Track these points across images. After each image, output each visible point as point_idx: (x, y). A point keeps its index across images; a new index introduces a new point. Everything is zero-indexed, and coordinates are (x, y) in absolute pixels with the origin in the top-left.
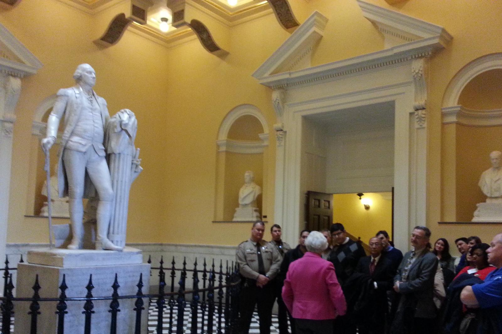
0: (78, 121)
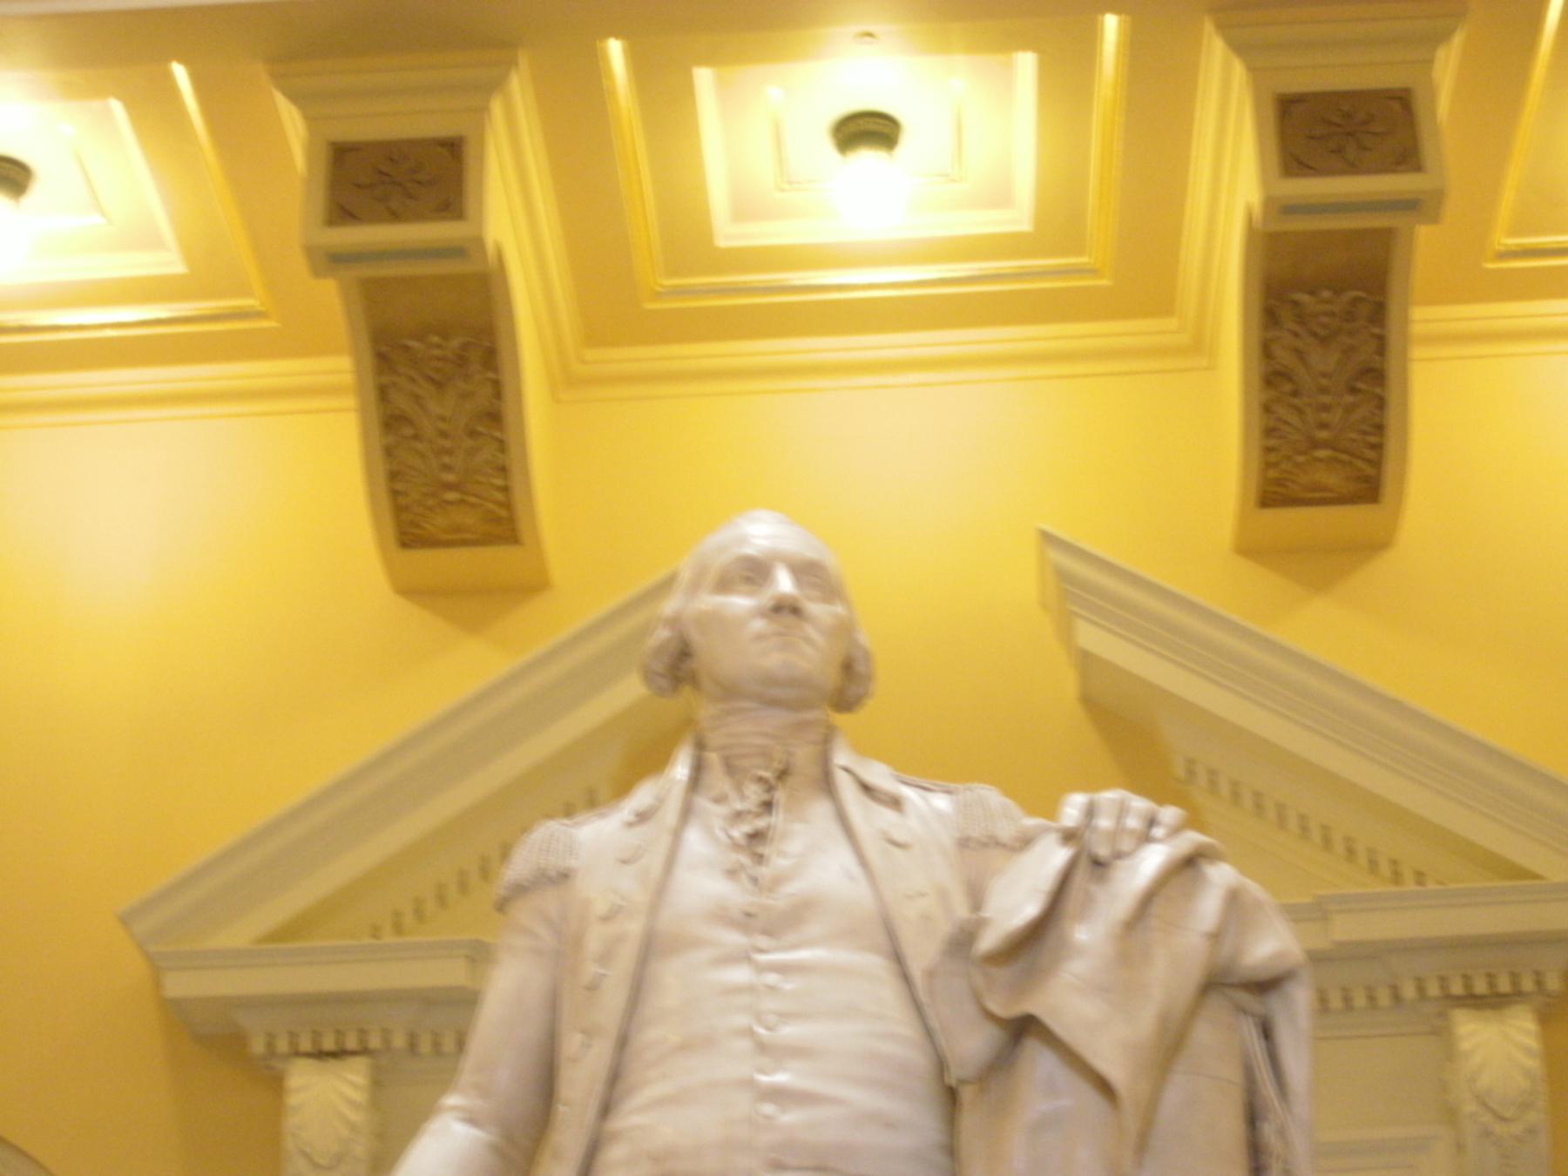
0: (615, 1084)
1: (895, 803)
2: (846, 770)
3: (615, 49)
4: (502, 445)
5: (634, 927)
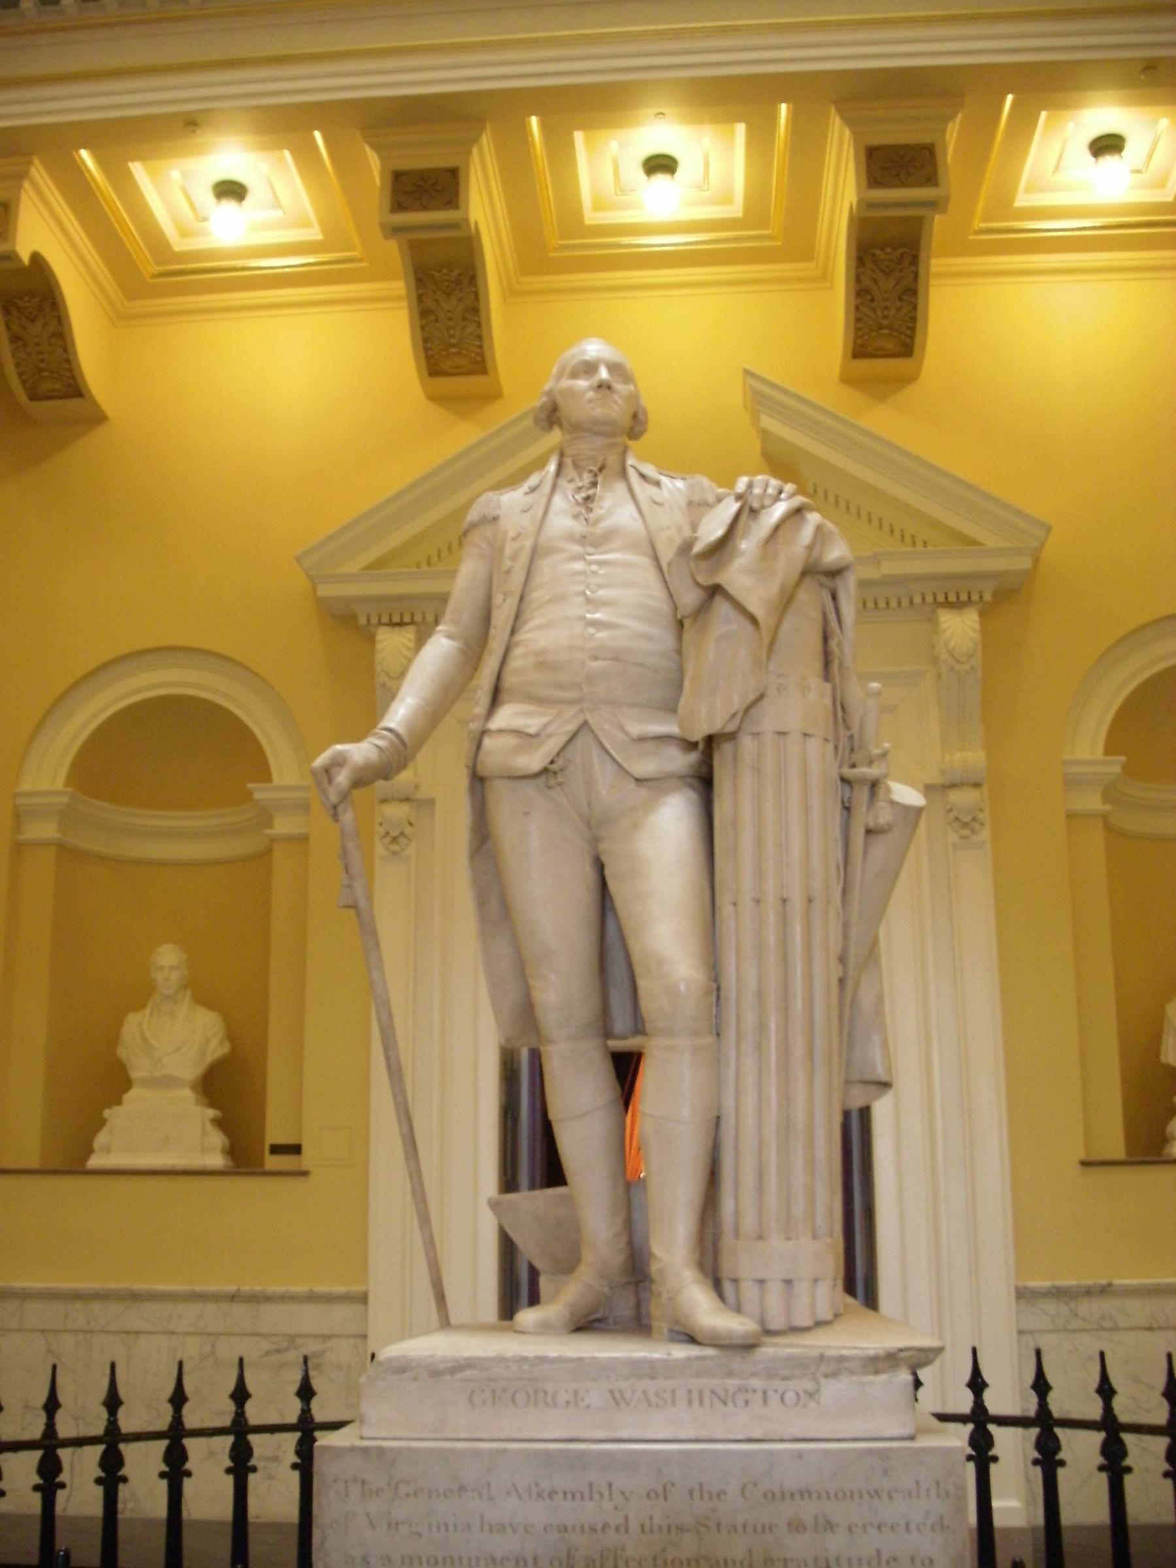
0: (518, 619)
1: (657, 484)
2: (631, 466)
3: (534, 121)
4: (479, 325)
5: (528, 544)
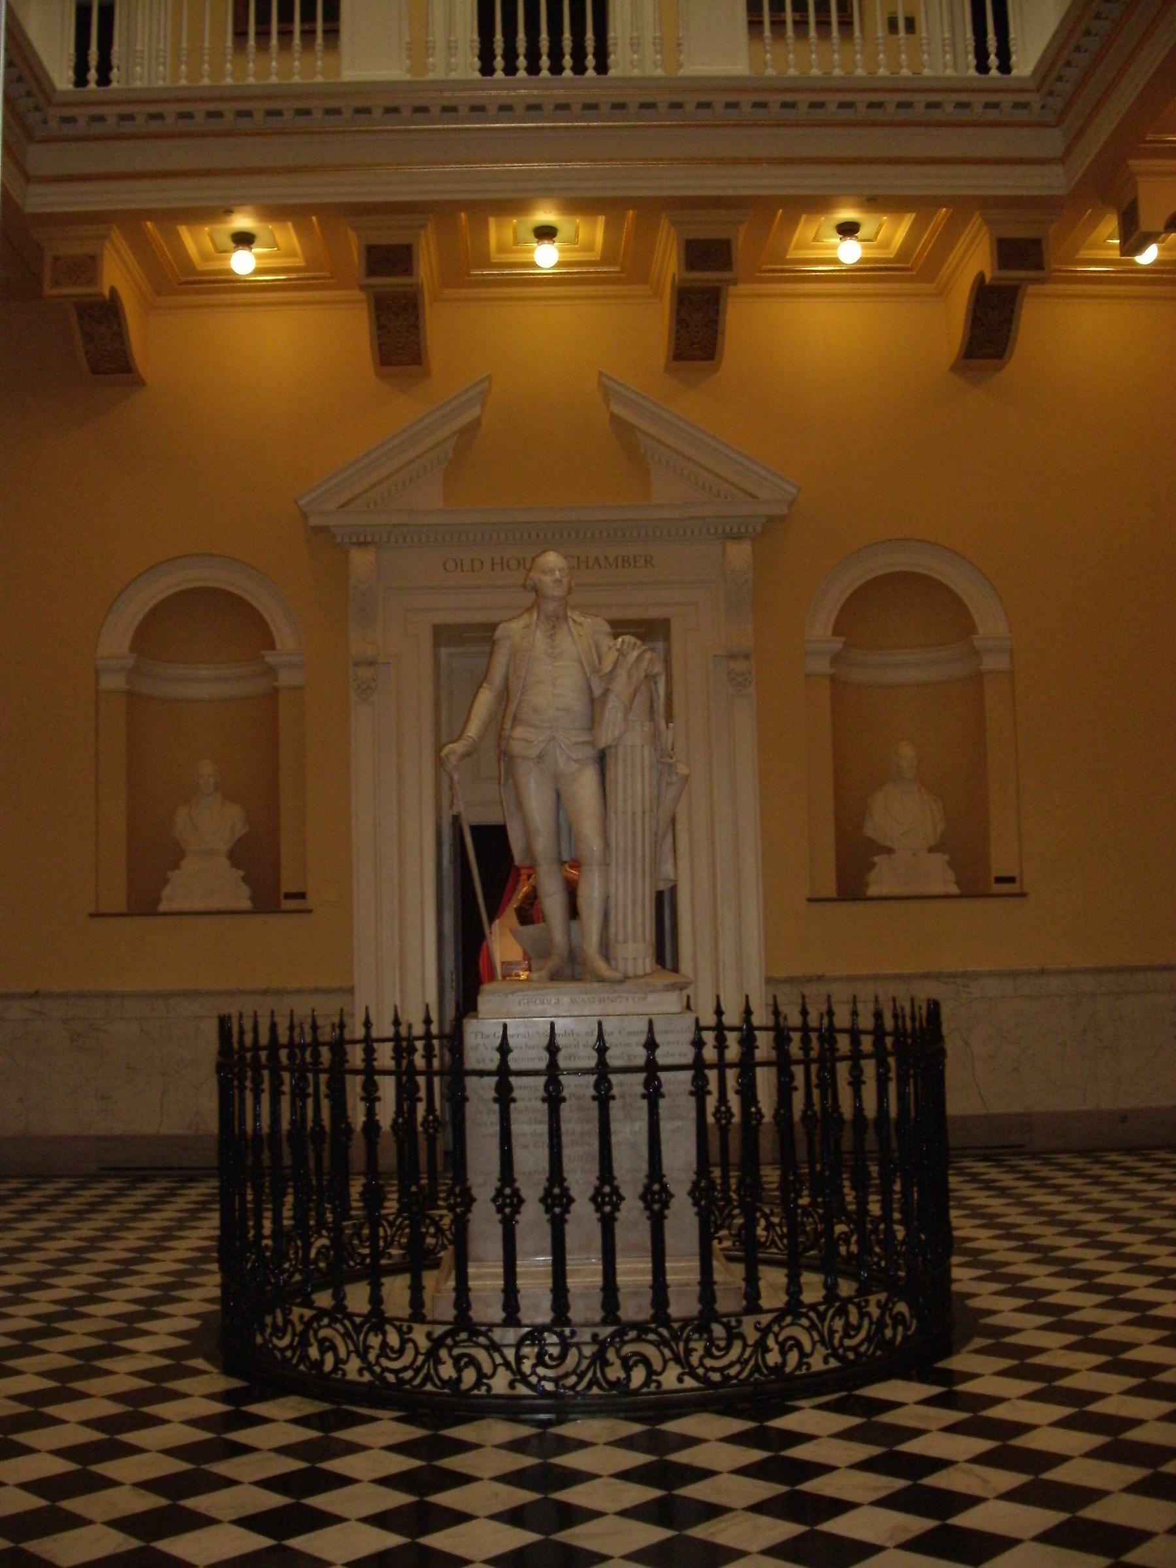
3: (463, 215)
